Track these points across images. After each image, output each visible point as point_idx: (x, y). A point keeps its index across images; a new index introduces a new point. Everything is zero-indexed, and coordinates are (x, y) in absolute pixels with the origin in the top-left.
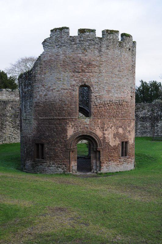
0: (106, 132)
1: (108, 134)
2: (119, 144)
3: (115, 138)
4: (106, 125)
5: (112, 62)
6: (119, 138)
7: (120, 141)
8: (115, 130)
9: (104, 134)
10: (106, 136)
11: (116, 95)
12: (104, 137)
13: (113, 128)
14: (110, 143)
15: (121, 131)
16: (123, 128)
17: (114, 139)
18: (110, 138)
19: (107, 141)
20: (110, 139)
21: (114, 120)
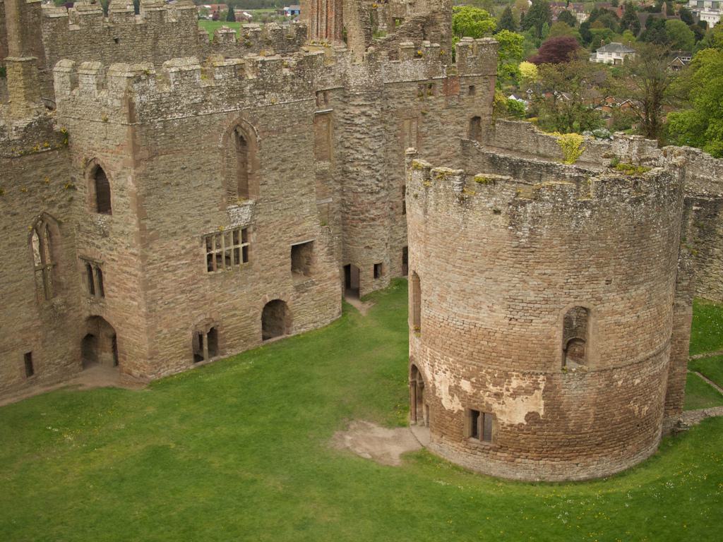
0: (436, 376)
1: (441, 382)
2: (460, 411)
3: (453, 396)
4: (436, 364)
5: (447, 238)
6: (462, 400)
7: (463, 406)
8: (452, 380)
9: (434, 379)
10: (437, 384)
11: (455, 310)
12: (434, 385)
13: (448, 373)
14: (443, 402)
15: (466, 386)
16: (472, 383)
17: (450, 397)
18: (443, 391)
19: (437, 394)
20: (443, 394)
21: (451, 359)
